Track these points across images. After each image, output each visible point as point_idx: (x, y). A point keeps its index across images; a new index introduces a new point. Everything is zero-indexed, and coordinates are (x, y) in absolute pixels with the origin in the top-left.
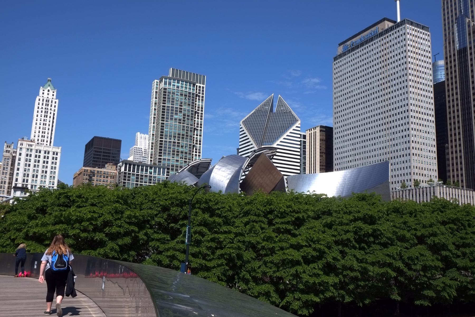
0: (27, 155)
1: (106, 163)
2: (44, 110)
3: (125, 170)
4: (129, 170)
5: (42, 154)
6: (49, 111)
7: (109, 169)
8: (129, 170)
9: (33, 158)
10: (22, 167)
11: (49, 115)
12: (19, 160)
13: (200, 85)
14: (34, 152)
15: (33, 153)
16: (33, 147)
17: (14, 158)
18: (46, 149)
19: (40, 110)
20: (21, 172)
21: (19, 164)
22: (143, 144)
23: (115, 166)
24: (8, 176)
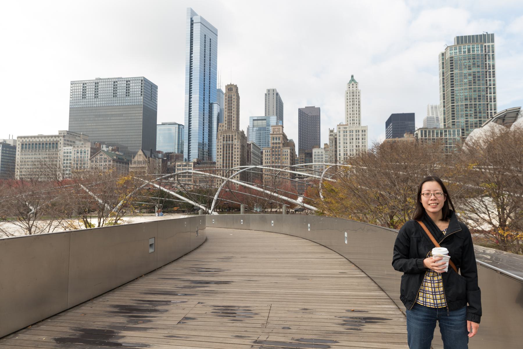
0: (344, 136)
1: (404, 133)
2: (351, 100)
3: (422, 136)
4: (426, 136)
5: (354, 133)
6: (355, 100)
7: (407, 138)
8: (426, 136)
9: (348, 137)
10: (342, 145)
11: (355, 103)
12: (339, 140)
13: (489, 44)
14: (348, 132)
15: (348, 133)
16: (348, 129)
17: (336, 138)
18: (357, 129)
19: (349, 101)
20: (342, 149)
21: (340, 143)
22: (435, 113)
23: (412, 135)
24: (334, 153)
